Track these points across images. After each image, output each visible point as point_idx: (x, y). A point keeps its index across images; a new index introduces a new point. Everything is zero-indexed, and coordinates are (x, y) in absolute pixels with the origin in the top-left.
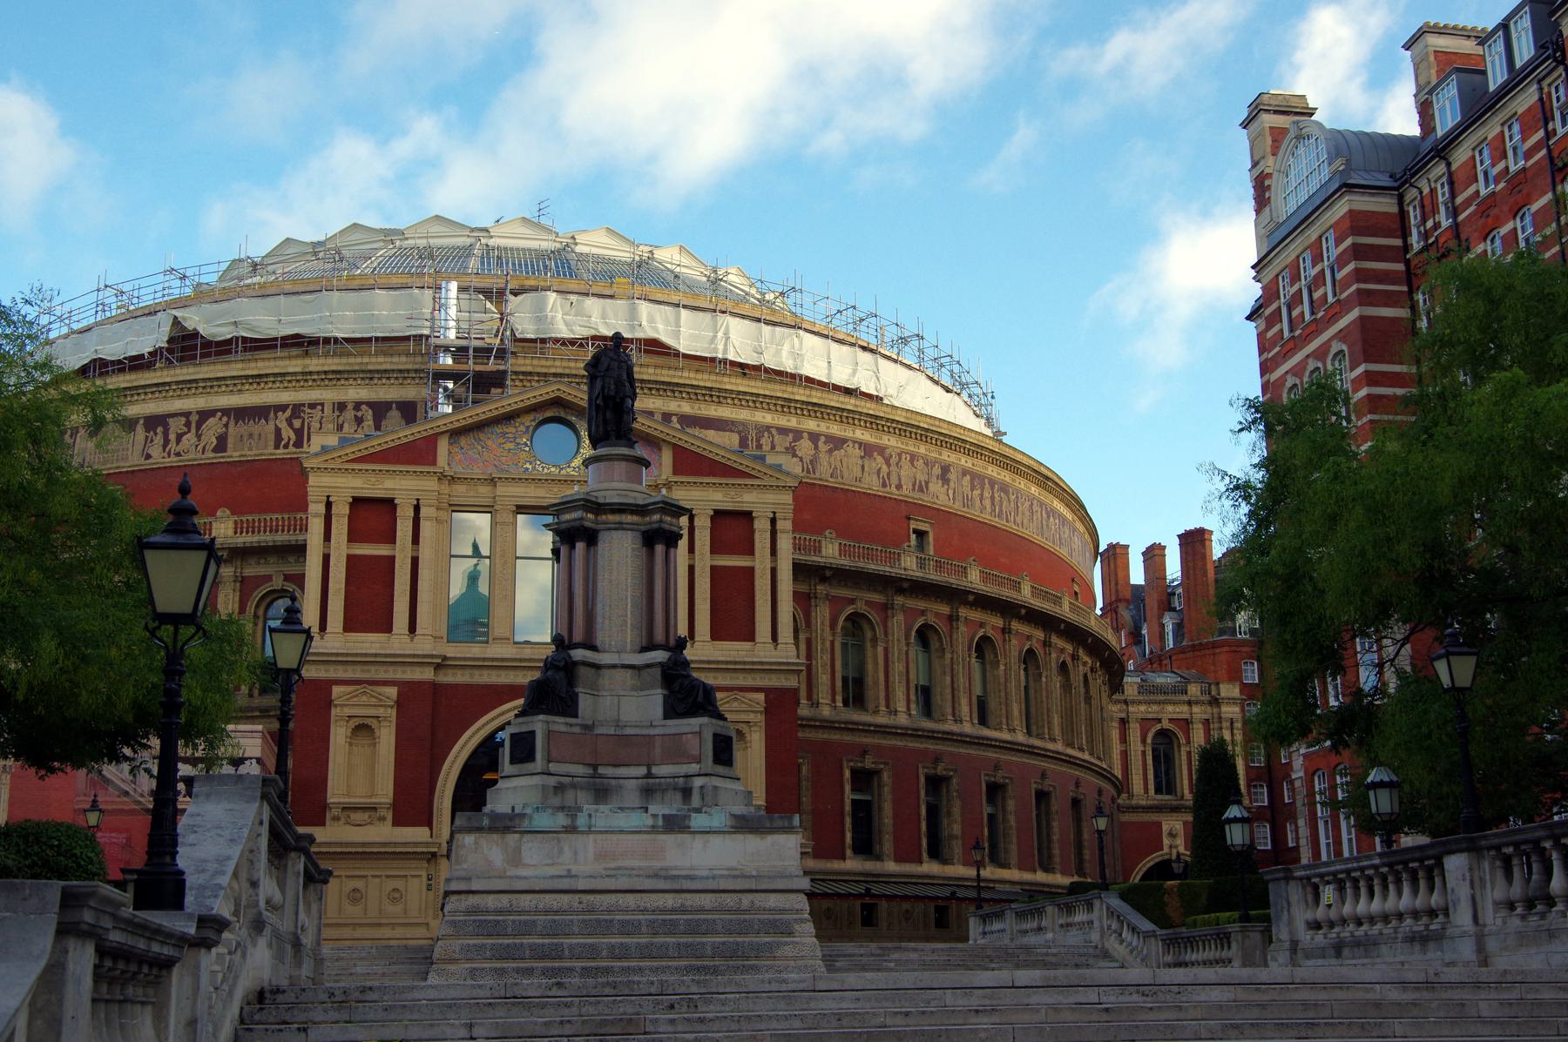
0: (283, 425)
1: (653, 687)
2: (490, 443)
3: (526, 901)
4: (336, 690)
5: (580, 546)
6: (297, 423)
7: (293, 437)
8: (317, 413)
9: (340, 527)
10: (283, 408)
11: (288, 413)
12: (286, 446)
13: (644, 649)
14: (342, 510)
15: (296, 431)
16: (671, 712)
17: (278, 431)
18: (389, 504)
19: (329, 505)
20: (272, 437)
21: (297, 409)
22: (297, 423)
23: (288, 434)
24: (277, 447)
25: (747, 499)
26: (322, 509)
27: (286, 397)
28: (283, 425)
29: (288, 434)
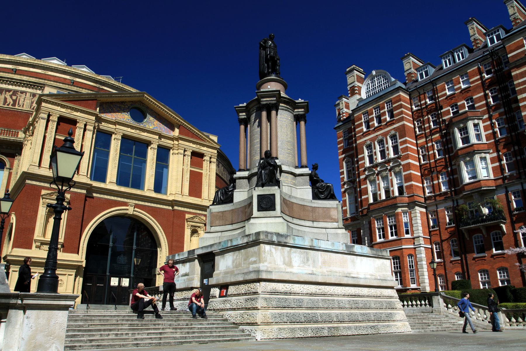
0: (8, 97)
1: (304, 185)
2: (114, 109)
3: (297, 288)
4: (43, 192)
5: (274, 113)
6: (14, 98)
7: (12, 102)
8: (23, 95)
9: (53, 126)
10: (9, 91)
11: (11, 93)
12: (8, 105)
13: (296, 167)
14: (54, 118)
15: (13, 100)
16: (316, 196)
17: (6, 99)
18: (73, 122)
19: (49, 116)
20: (3, 100)
21: (15, 92)
22: (14, 98)
23: (9, 100)
24: (4, 104)
25: (204, 150)
26: (46, 116)
27: (10, 87)
28: (8, 97)
29: (9, 100)
